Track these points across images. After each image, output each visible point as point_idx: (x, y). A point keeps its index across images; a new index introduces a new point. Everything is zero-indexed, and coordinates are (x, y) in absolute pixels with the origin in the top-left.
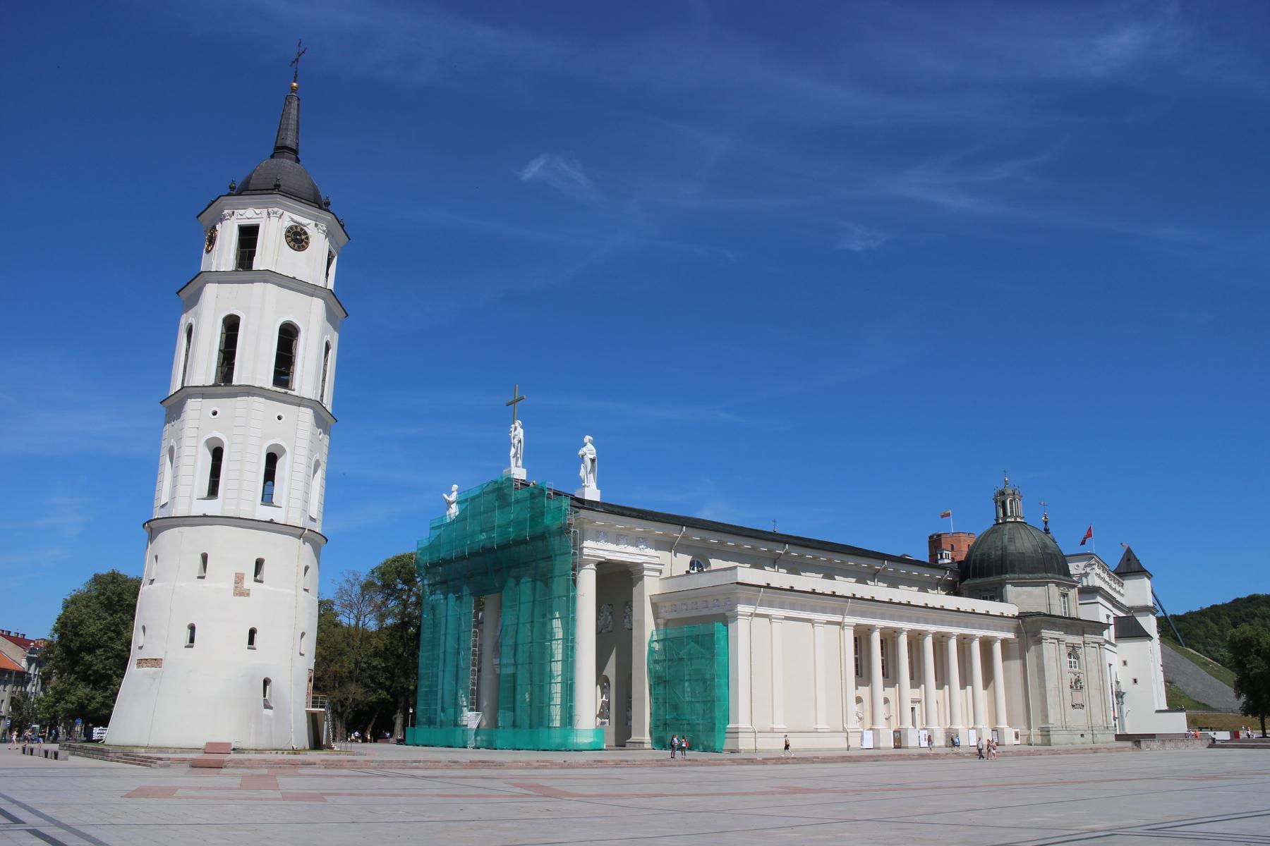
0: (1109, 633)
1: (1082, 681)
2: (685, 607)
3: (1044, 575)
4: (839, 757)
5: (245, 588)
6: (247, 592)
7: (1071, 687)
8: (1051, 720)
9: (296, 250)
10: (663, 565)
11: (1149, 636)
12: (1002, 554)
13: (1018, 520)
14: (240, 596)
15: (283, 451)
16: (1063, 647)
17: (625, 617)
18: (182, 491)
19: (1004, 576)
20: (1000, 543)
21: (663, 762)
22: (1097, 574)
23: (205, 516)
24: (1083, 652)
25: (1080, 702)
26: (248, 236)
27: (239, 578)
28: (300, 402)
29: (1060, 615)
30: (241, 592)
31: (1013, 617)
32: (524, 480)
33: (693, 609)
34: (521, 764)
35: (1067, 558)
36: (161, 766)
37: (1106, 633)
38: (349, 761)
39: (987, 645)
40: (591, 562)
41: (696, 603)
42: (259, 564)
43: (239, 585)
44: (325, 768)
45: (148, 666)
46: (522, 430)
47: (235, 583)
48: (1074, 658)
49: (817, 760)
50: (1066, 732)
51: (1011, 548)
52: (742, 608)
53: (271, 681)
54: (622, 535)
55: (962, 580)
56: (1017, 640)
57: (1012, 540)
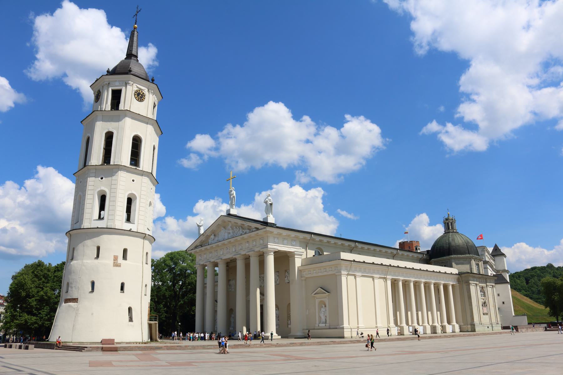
1: (487, 302)
2: (315, 271)
3: (468, 255)
4: (395, 339)
5: (119, 262)
6: (120, 264)
7: (482, 305)
8: (475, 321)
9: (139, 101)
10: (303, 252)
12: (449, 246)
13: (455, 231)
14: (116, 267)
15: (136, 198)
16: (478, 287)
17: (285, 277)
18: (86, 216)
19: (450, 256)
20: (448, 242)
21: (321, 343)
22: (487, 255)
23: (98, 228)
25: (486, 312)
26: (117, 95)
27: (116, 258)
28: (143, 173)
30: (116, 265)
31: (456, 274)
32: (236, 215)
33: (319, 272)
34: (258, 346)
35: (477, 248)
36: (87, 351)
38: (177, 346)
39: (446, 287)
40: (271, 251)
41: (320, 269)
42: (125, 251)
43: (116, 261)
44: (167, 350)
45: (70, 302)
46: (235, 192)
47: (114, 260)
48: (483, 292)
49: (387, 340)
50: (481, 326)
51: (453, 244)
52: (343, 272)
54: (285, 239)
56: (458, 285)
57: (453, 240)
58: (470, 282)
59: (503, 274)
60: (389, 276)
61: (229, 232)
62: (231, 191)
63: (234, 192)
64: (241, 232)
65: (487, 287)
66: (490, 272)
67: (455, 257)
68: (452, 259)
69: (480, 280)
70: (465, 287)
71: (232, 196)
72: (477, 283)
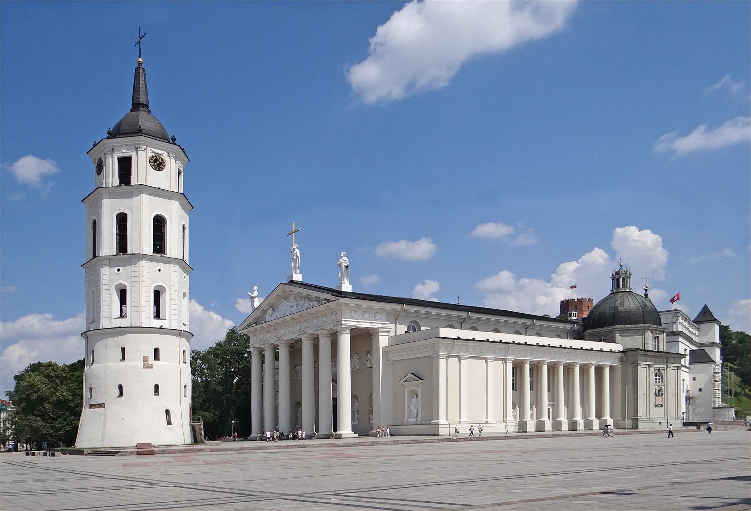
0: (685, 360)
11: (714, 362)
15: (164, 290)
24: (666, 373)
27: (145, 359)
28: (171, 261)
29: (650, 348)
30: (147, 366)
31: (619, 352)
32: (301, 282)
37: (682, 361)
39: (599, 370)
42: (156, 351)
43: (146, 363)
46: (298, 250)
51: (621, 309)
53: (169, 410)
55: (585, 331)
57: (622, 303)
58: (639, 362)
59: (707, 350)
60: (510, 356)
61: (291, 304)
62: (294, 249)
63: (297, 252)
64: (307, 305)
65: (667, 369)
66: (683, 347)
67: (621, 328)
68: (615, 331)
69: (657, 360)
70: (630, 369)
71: (295, 257)
72: (651, 364)
